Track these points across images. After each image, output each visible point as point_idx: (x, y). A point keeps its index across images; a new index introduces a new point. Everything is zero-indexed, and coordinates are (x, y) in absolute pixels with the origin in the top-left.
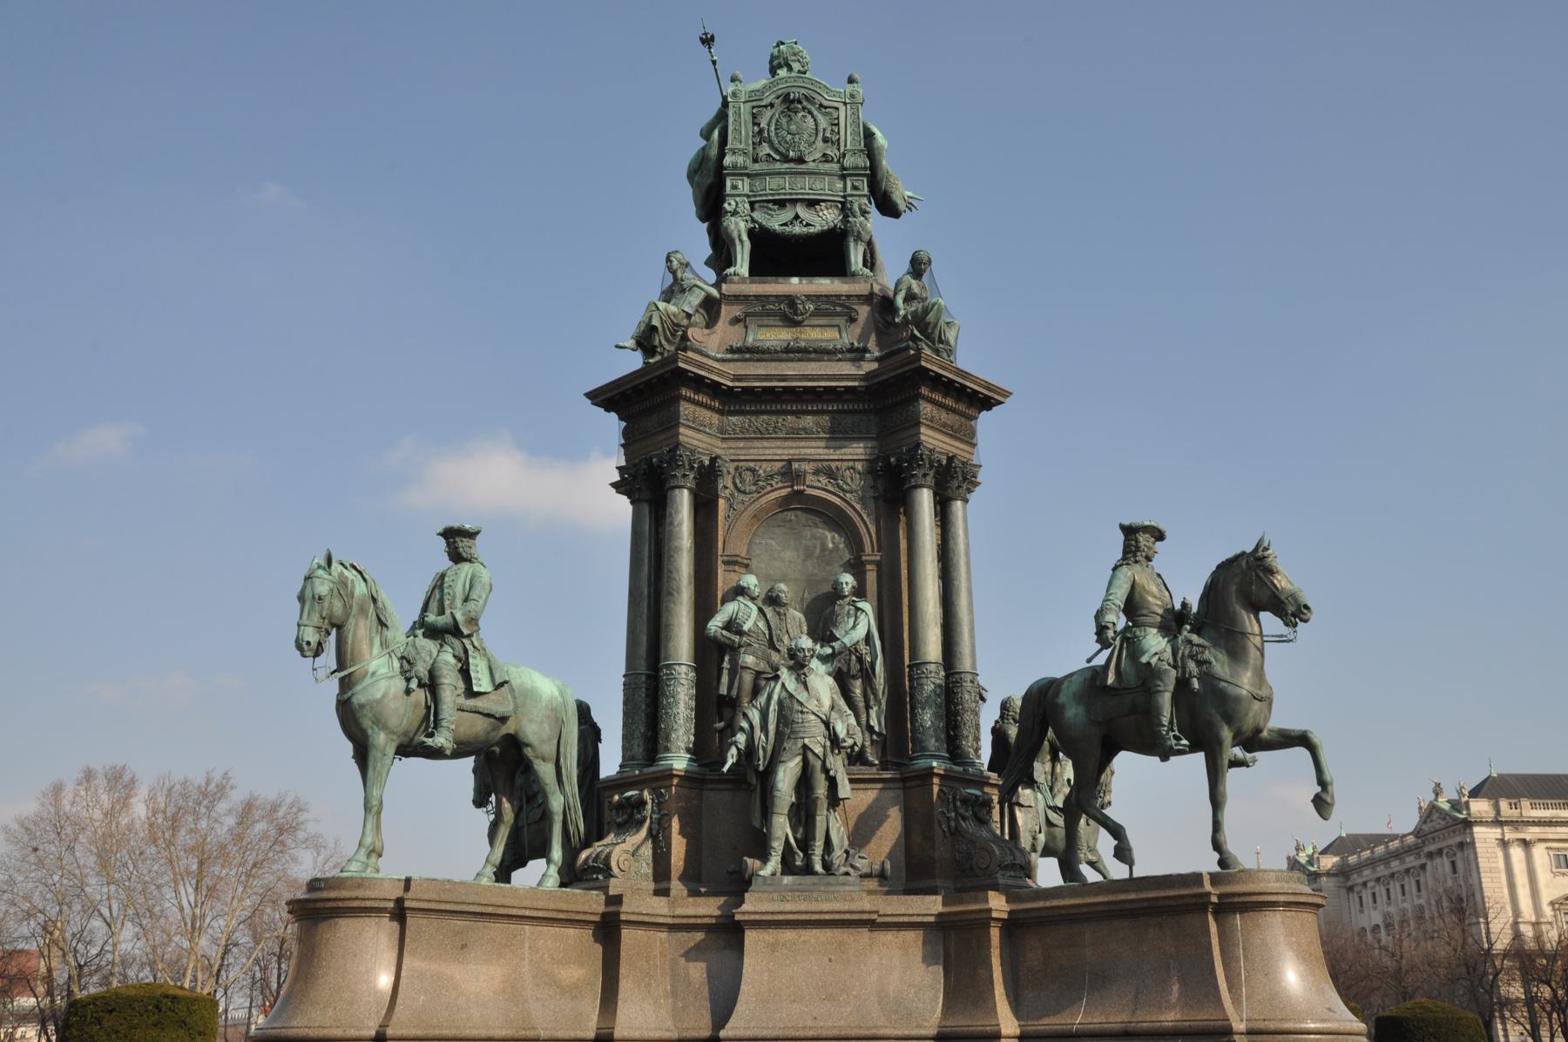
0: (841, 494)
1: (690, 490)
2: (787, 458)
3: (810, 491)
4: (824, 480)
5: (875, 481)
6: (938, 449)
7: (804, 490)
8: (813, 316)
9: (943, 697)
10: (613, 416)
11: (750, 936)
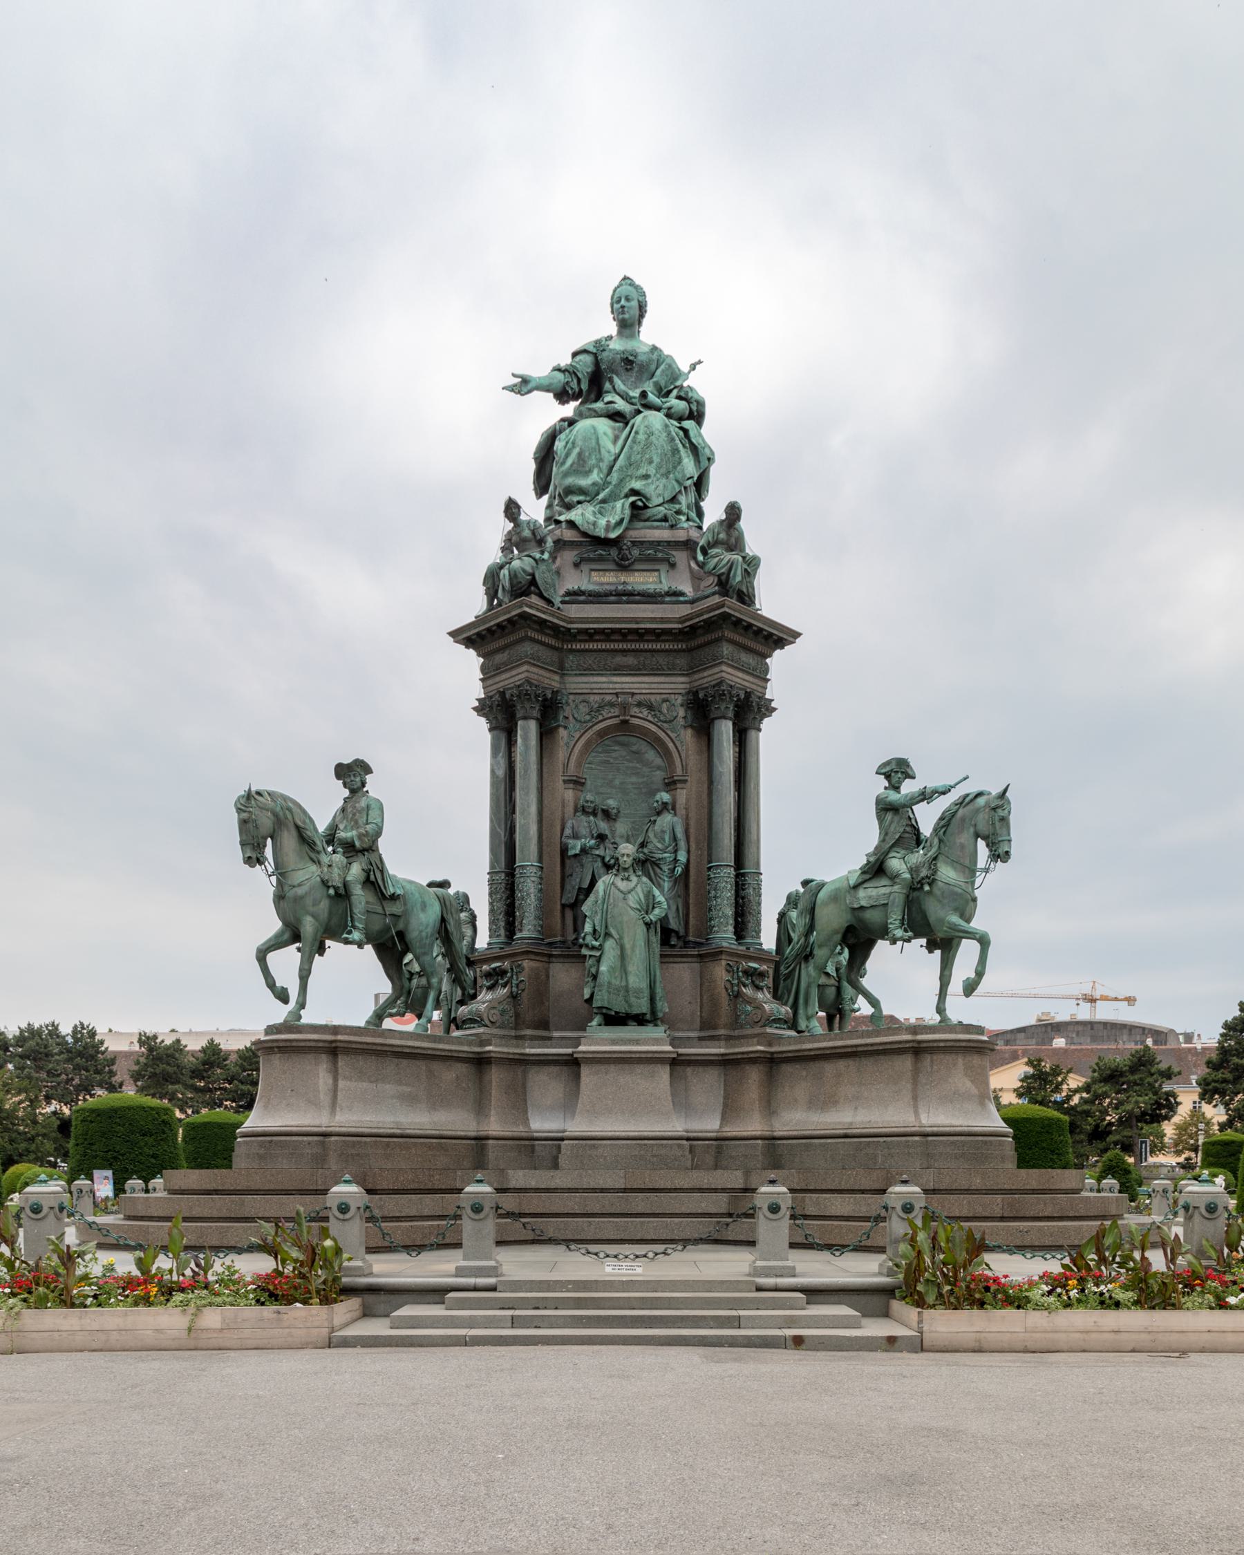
0: (659, 724)
1: (537, 719)
2: (615, 691)
4: (645, 713)
5: (686, 711)
6: (737, 685)
7: (628, 720)
8: (639, 561)
9: (733, 892)
10: (472, 653)
11: (585, 1071)
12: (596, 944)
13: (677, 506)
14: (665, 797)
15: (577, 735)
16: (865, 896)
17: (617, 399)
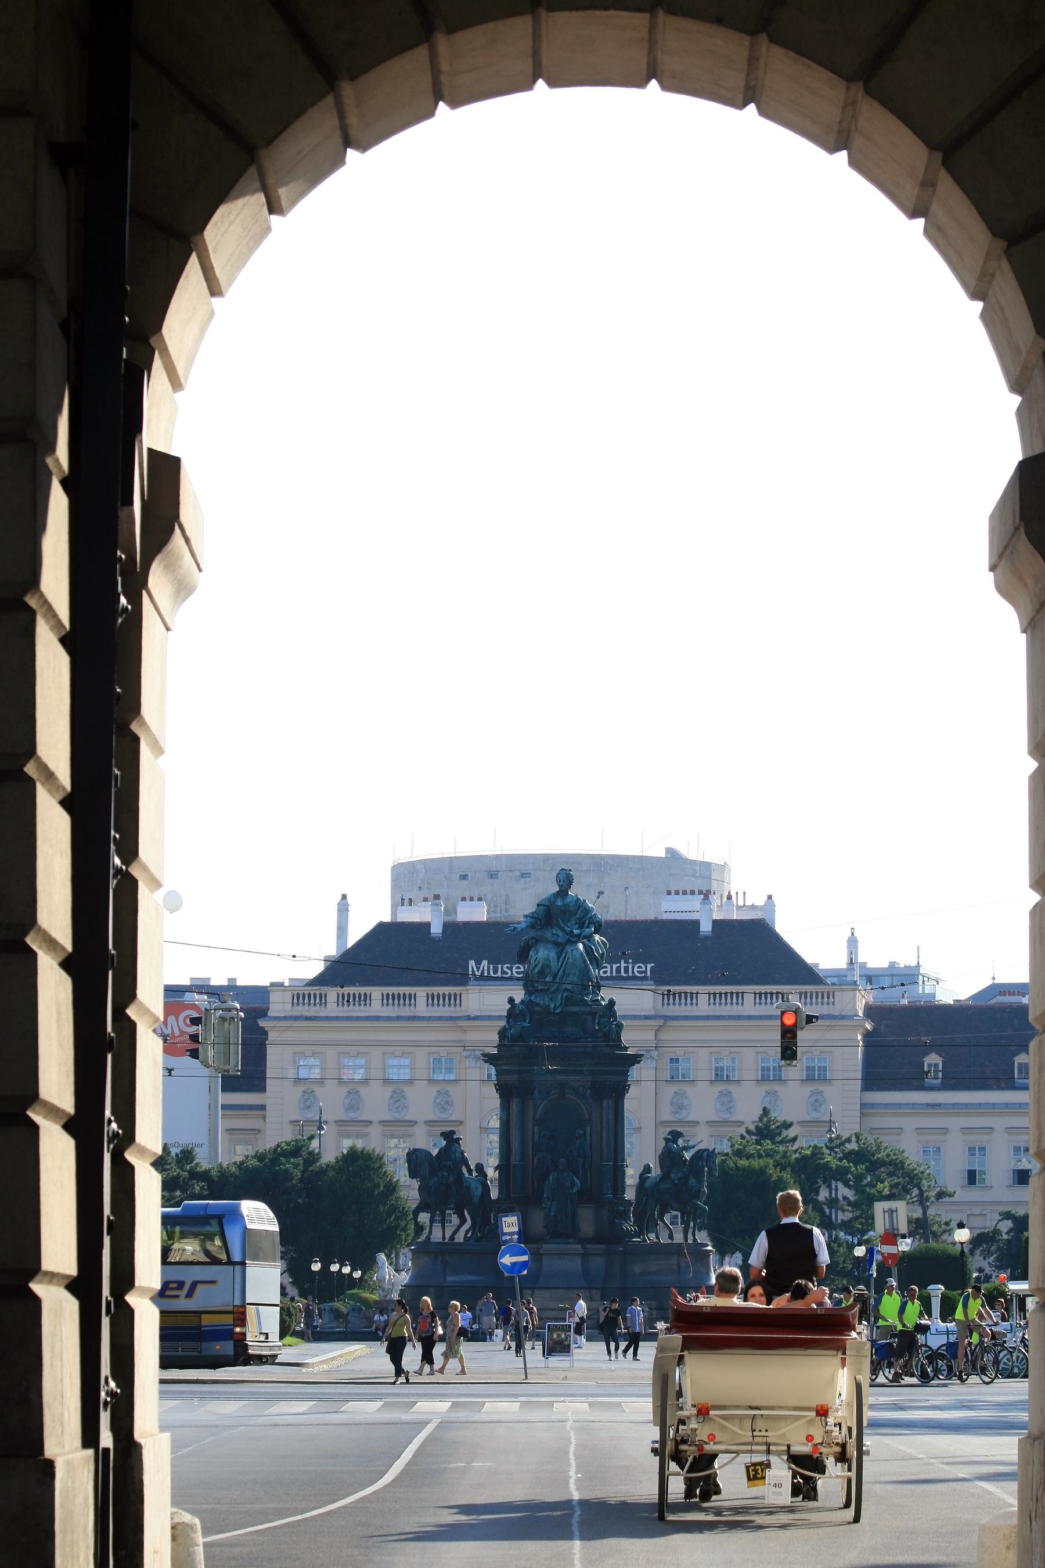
3: (567, 1096)
11: (544, 1258)
12: (549, 1203)
13: (587, 992)
14: (581, 1132)
15: (540, 1102)
16: (663, 1186)
17: (560, 933)
